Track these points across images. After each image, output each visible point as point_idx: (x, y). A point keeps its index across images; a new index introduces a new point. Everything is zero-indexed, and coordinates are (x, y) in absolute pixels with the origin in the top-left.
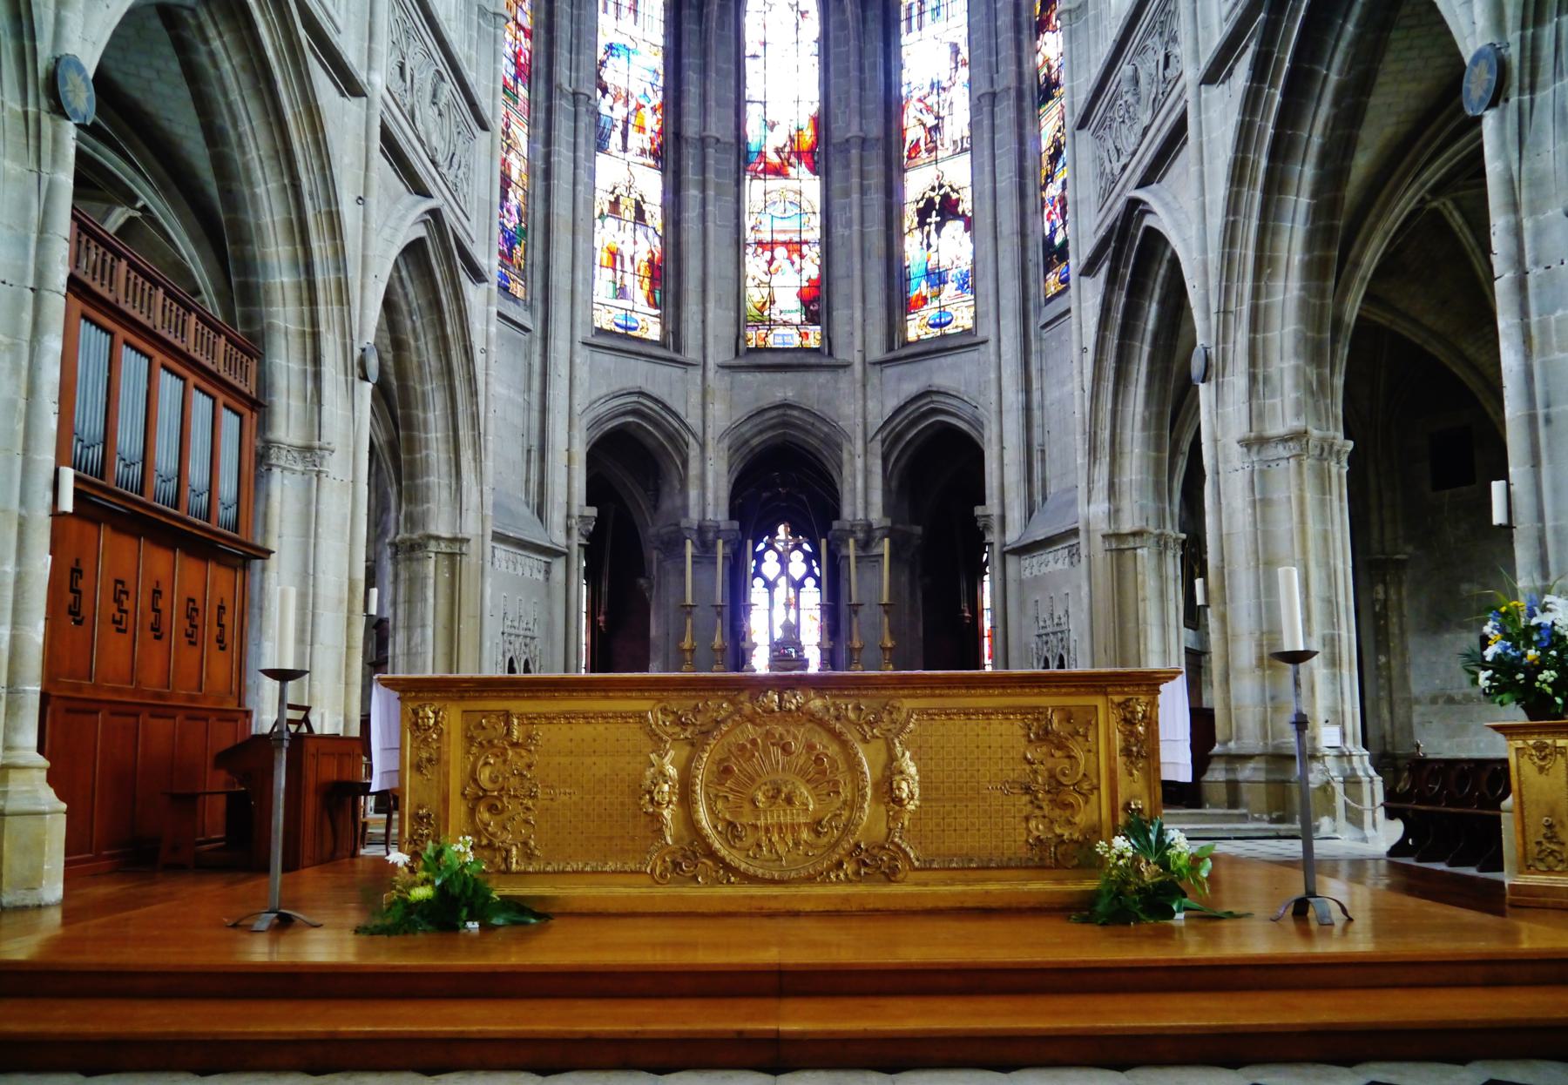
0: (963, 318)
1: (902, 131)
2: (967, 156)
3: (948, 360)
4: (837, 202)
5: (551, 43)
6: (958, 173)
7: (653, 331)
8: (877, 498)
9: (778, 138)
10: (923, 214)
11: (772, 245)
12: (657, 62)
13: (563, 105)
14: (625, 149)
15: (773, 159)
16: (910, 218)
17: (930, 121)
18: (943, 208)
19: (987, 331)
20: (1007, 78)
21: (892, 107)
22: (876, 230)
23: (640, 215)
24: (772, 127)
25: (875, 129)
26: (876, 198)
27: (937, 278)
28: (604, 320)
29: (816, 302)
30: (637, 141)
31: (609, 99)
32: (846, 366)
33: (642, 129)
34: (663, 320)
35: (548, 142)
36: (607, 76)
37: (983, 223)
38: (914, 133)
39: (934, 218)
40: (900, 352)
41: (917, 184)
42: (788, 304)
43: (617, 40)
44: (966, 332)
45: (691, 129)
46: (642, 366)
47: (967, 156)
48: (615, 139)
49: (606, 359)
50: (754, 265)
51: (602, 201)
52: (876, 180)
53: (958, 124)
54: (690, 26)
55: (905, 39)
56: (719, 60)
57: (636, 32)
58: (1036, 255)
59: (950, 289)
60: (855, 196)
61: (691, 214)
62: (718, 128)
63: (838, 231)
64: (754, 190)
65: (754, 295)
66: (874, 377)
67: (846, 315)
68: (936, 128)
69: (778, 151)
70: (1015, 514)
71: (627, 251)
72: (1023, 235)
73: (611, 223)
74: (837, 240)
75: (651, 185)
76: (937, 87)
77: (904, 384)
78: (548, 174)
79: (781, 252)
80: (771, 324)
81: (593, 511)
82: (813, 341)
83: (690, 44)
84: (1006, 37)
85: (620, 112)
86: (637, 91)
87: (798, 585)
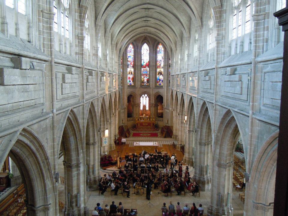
0: (162, 85)
1: (157, 64)
2: (163, 69)
3: (160, 89)
4: (150, 72)
5: (124, 60)
6: (162, 70)
7: (133, 84)
8: (154, 101)
9: (145, 64)
10: (159, 73)
11: (144, 75)
12: (132, 57)
13: (125, 66)
14: (130, 67)
15: (144, 66)
16: (158, 74)
17: (160, 64)
18: (160, 73)
19: (164, 87)
20: (166, 64)
21: (156, 61)
22: (154, 75)
23: (132, 73)
24: (144, 62)
25: (154, 64)
26: (154, 71)
27: (160, 80)
28: (128, 84)
29: (148, 80)
30: (131, 66)
31: (129, 62)
32: (151, 88)
33: (132, 64)
34: (134, 83)
35: (124, 70)
36: (128, 60)
37: (164, 75)
38: (158, 65)
39: (160, 74)
40: (156, 87)
41: (158, 70)
42: (146, 81)
43: (129, 55)
44: (162, 86)
45: (136, 64)
46: (132, 89)
47: (163, 69)
48: (129, 66)
49: (129, 89)
50: (143, 77)
51: (128, 72)
52: (154, 70)
53: (162, 65)
54: (136, 53)
55: (158, 54)
56: (140, 56)
57: (131, 54)
58: (168, 82)
59: (161, 82)
60: (152, 71)
61: (136, 73)
62: (139, 64)
63: (151, 74)
64: (142, 69)
65: (143, 80)
66: (154, 90)
67: (151, 83)
68: (160, 65)
69: (145, 65)
70: (166, 105)
71: (130, 77)
72: (167, 79)
73: (129, 75)
74: (150, 75)
75: (132, 70)
76: (160, 61)
77: (156, 90)
78: (124, 73)
79: (145, 76)
80: (144, 83)
81: (128, 104)
82: (148, 85)
83: (136, 55)
84: (167, 59)
85: (130, 63)
86: (131, 60)
87: (146, 97)
